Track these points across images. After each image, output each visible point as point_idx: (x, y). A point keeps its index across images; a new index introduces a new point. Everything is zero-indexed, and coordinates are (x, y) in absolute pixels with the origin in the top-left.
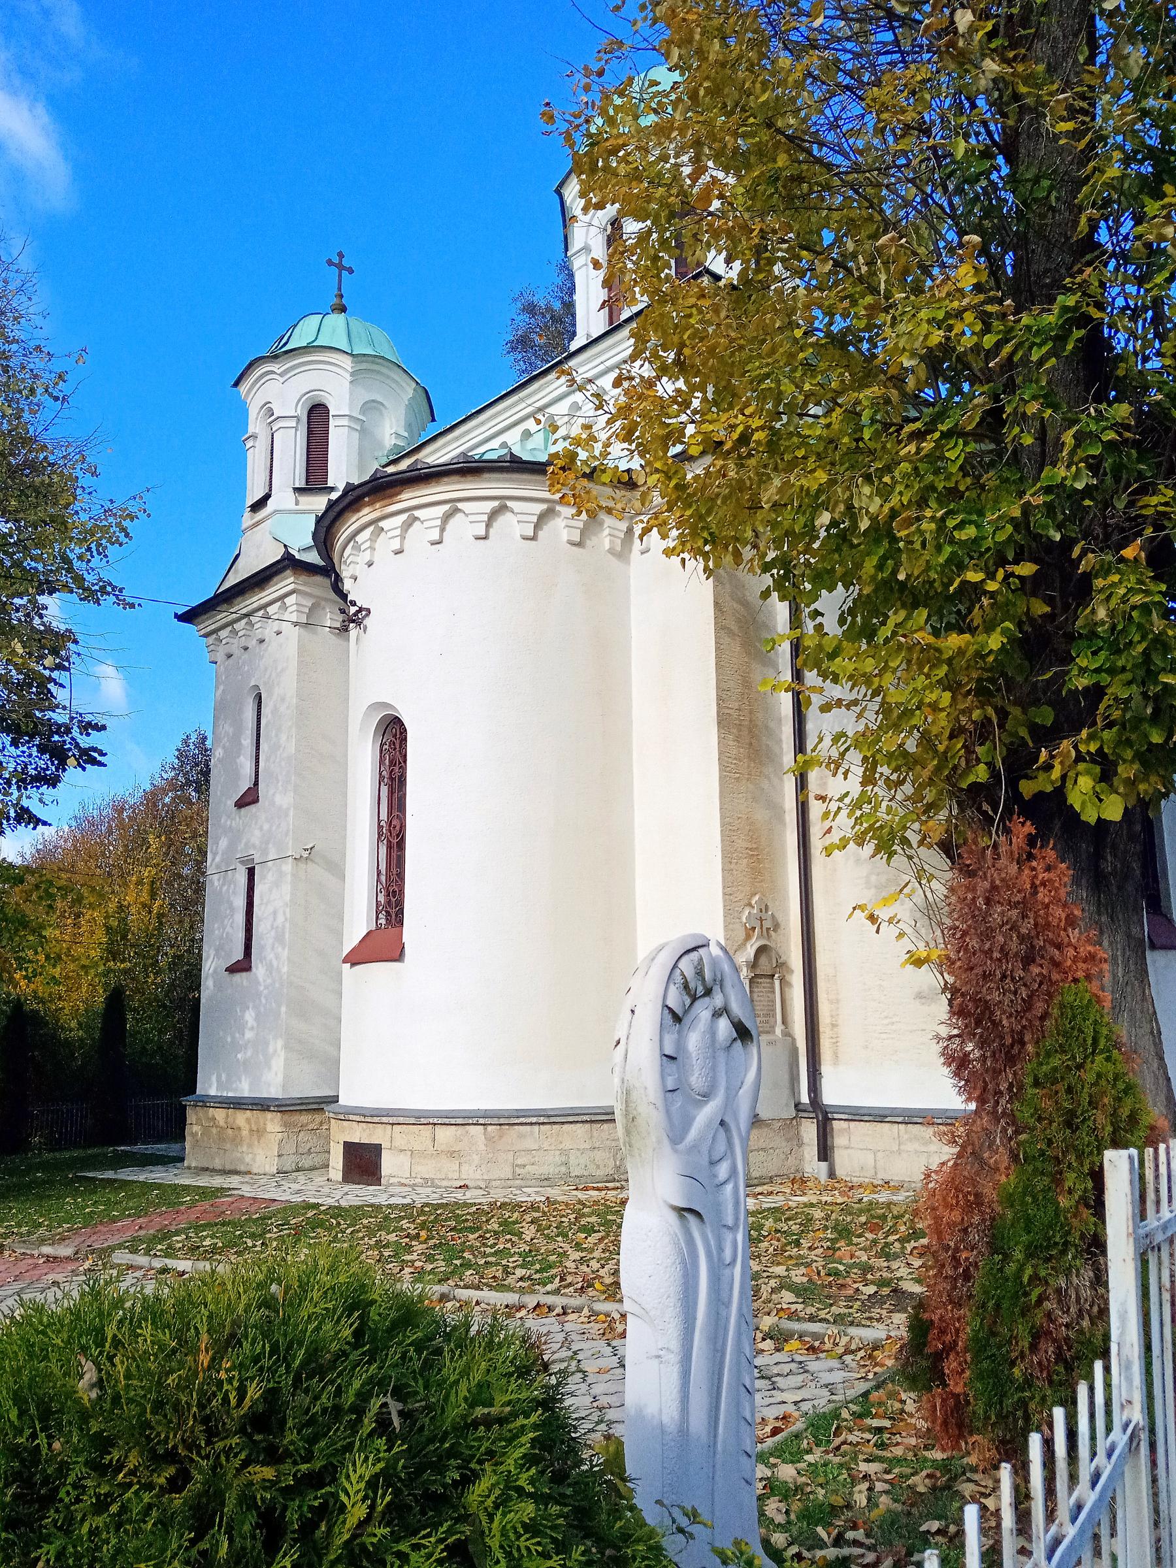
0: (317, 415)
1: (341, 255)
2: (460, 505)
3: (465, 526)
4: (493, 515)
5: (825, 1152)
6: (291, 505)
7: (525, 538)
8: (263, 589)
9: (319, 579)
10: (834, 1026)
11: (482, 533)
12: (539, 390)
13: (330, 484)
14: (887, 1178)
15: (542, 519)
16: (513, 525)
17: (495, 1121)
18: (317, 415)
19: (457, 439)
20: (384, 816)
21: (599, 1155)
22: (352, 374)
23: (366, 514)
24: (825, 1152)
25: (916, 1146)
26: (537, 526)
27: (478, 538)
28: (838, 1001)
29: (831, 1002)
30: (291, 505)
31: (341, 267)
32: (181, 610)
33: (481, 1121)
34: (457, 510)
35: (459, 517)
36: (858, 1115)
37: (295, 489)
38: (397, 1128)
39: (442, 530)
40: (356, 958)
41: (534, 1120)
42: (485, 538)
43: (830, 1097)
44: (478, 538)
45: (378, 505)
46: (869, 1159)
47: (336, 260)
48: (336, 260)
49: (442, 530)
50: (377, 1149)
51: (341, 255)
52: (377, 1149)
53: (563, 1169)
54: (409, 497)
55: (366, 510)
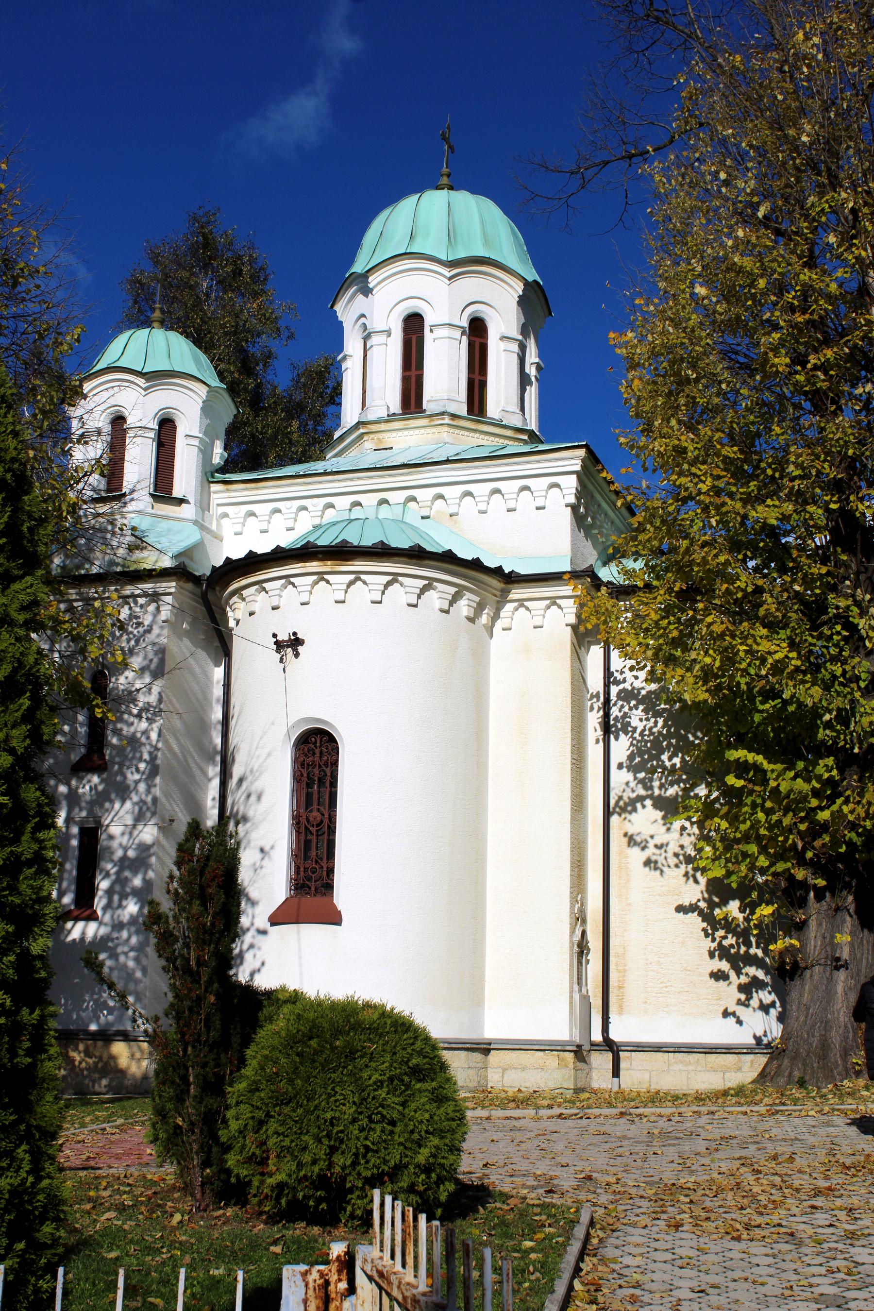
2: (400, 578)
3: (400, 595)
4: (423, 590)
5: (616, 1073)
6: (150, 510)
9: (190, 586)
10: (620, 988)
12: (407, 474)
13: (177, 493)
14: (658, 1088)
15: (455, 599)
16: (436, 599)
21: (470, 1071)
23: (314, 566)
24: (616, 1073)
25: (680, 1066)
26: (451, 603)
27: (409, 605)
28: (625, 971)
29: (619, 971)
30: (150, 510)
34: (396, 581)
35: (396, 585)
36: (640, 1048)
39: (383, 593)
40: (275, 920)
42: (416, 606)
43: (614, 1035)
44: (409, 605)
45: (329, 563)
46: (646, 1076)
49: (383, 593)
54: (358, 566)
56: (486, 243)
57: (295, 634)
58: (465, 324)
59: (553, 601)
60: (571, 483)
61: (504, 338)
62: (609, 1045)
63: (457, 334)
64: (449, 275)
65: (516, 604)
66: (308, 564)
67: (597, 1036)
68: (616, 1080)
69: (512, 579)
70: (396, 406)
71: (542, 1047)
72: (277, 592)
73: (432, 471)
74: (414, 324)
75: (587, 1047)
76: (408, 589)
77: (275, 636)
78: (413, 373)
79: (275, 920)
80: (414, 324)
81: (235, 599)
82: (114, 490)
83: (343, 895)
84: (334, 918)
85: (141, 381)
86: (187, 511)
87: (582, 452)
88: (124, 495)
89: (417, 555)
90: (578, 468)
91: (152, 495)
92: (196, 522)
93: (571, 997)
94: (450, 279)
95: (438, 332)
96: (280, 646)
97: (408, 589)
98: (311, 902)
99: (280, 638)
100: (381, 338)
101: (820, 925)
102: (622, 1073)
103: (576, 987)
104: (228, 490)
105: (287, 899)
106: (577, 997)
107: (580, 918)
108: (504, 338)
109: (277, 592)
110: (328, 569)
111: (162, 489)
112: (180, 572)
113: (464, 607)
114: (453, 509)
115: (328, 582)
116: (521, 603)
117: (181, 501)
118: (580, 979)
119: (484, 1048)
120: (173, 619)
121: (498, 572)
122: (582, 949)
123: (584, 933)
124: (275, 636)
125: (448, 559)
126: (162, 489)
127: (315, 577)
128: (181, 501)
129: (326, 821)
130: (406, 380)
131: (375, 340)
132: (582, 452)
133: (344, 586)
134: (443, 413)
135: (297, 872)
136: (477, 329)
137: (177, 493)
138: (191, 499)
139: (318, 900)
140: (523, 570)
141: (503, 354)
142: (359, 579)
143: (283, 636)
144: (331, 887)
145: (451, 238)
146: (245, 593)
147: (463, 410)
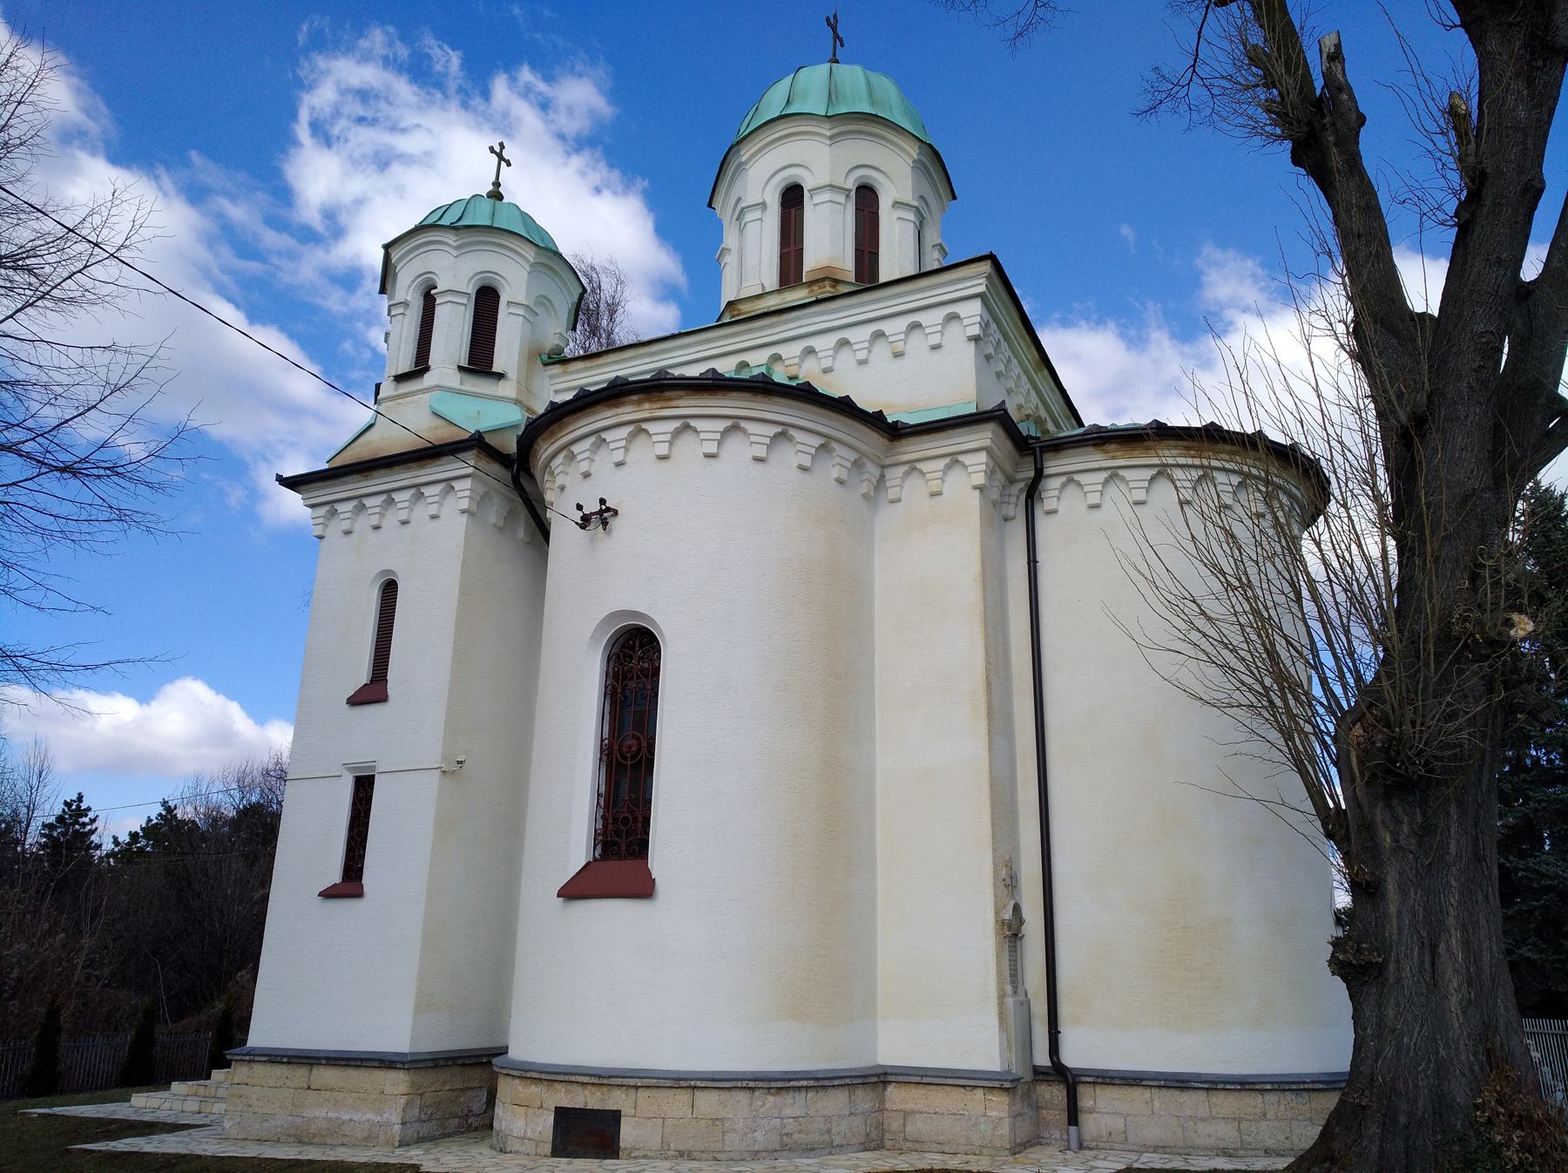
0: (486, 301)
1: (502, 146)
2: (743, 424)
7: (803, 468)
8: (423, 467)
9: (495, 468)
11: (761, 451)
13: (496, 368)
17: (765, 1085)
18: (486, 301)
19: (652, 354)
20: (606, 735)
21: (857, 1122)
22: (531, 265)
23: (628, 412)
31: (501, 157)
32: (288, 473)
33: (751, 1084)
36: (1107, 1079)
37: (461, 368)
38: (643, 1094)
40: (573, 891)
41: (804, 1083)
47: (497, 149)
48: (497, 149)
50: (615, 1116)
51: (502, 146)
52: (615, 1116)
53: (826, 1137)
54: (688, 406)
55: (629, 408)
56: (873, 101)
57: (602, 501)
58: (851, 184)
59: (954, 460)
60: (972, 311)
61: (897, 204)
62: (1058, 1072)
63: (841, 199)
64: (828, 133)
65: (906, 468)
66: (619, 411)
67: (1042, 1059)
68: (1072, 1128)
69: (896, 432)
70: (771, 279)
71: (961, 1082)
72: (587, 454)
73: (798, 319)
74: (793, 197)
75: (1028, 1077)
76: (753, 438)
77: (579, 507)
78: (793, 248)
79: (573, 891)
80: (793, 197)
81: (547, 477)
82: (421, 366)
83: (663, 855)
84: (643, 889)
85: (450, 238)
86: (507, 389)
87: (986, 267)
88: (427, 369)
89: (763, 387)
90: (982, 289)
91: (461, 368)
92: (517, 402)
93: (1001, 1004)
94: (831, 138)
95: (818, 198)
96: (585, 521)
97: (753, 438)
98: (621, 868)
99: (587, 511)
100: (756, 214)
101: (1403, 891)
102: (1083, 1117)
103: (1009, 989)
104: (565, 373)
105: (588, 864)
106: (1010, 1001)
107: (1009, 882)
108: (897, 204)
109: (587, 454)
110: (646, 415)
111: (480, 361)
112: (478, 443)
113: (833, 468)
114: (826, 363)
115: (646, 431)
116: (912, 467)
117: (500, 376)
118: (1013, 974)
119: (879, 1079)
120: (474, 509)
121: (875, 420)
122: (1011, 932)
123: (1017, 909)
124: (579, 507)
125: (805, 394)
126: (480, 361)
127: (630, 428)
128: (500, 376)
129: (644, 751)
130: (783, 257)
131: (749, 216)
132: (986, 267)
133: (668, 437)
134: (823, 279)
135: (605, 825)
136: (866, 199)
137: (496, 368)
138: (512, 374)
139: (630, 864)
140: (912, 420)
141: (897, 225)
142: (688, 427)
143: (592, 507)
144: (644, 845)
145: (832, 95)
146: (554, 464)
147: (851, 277)
